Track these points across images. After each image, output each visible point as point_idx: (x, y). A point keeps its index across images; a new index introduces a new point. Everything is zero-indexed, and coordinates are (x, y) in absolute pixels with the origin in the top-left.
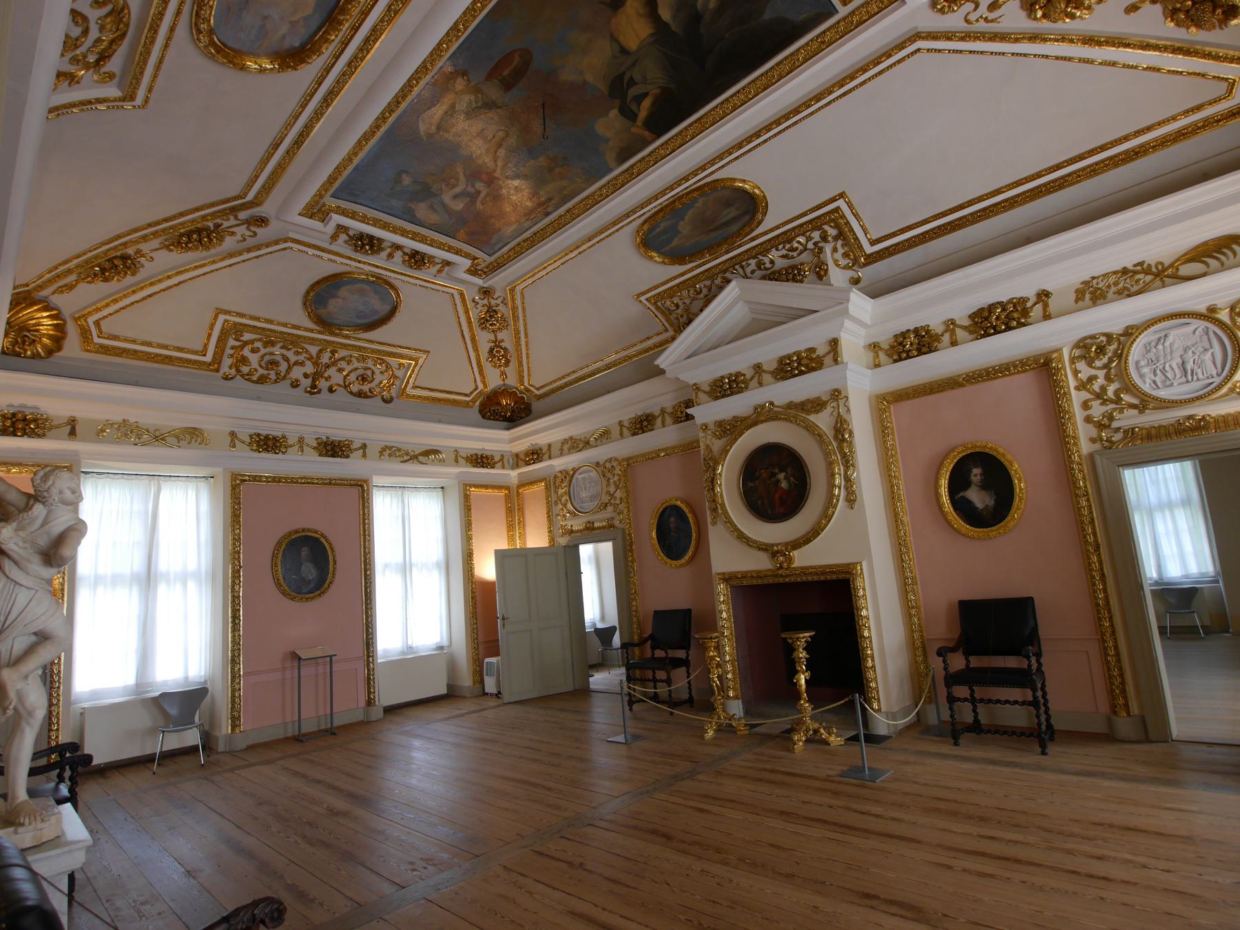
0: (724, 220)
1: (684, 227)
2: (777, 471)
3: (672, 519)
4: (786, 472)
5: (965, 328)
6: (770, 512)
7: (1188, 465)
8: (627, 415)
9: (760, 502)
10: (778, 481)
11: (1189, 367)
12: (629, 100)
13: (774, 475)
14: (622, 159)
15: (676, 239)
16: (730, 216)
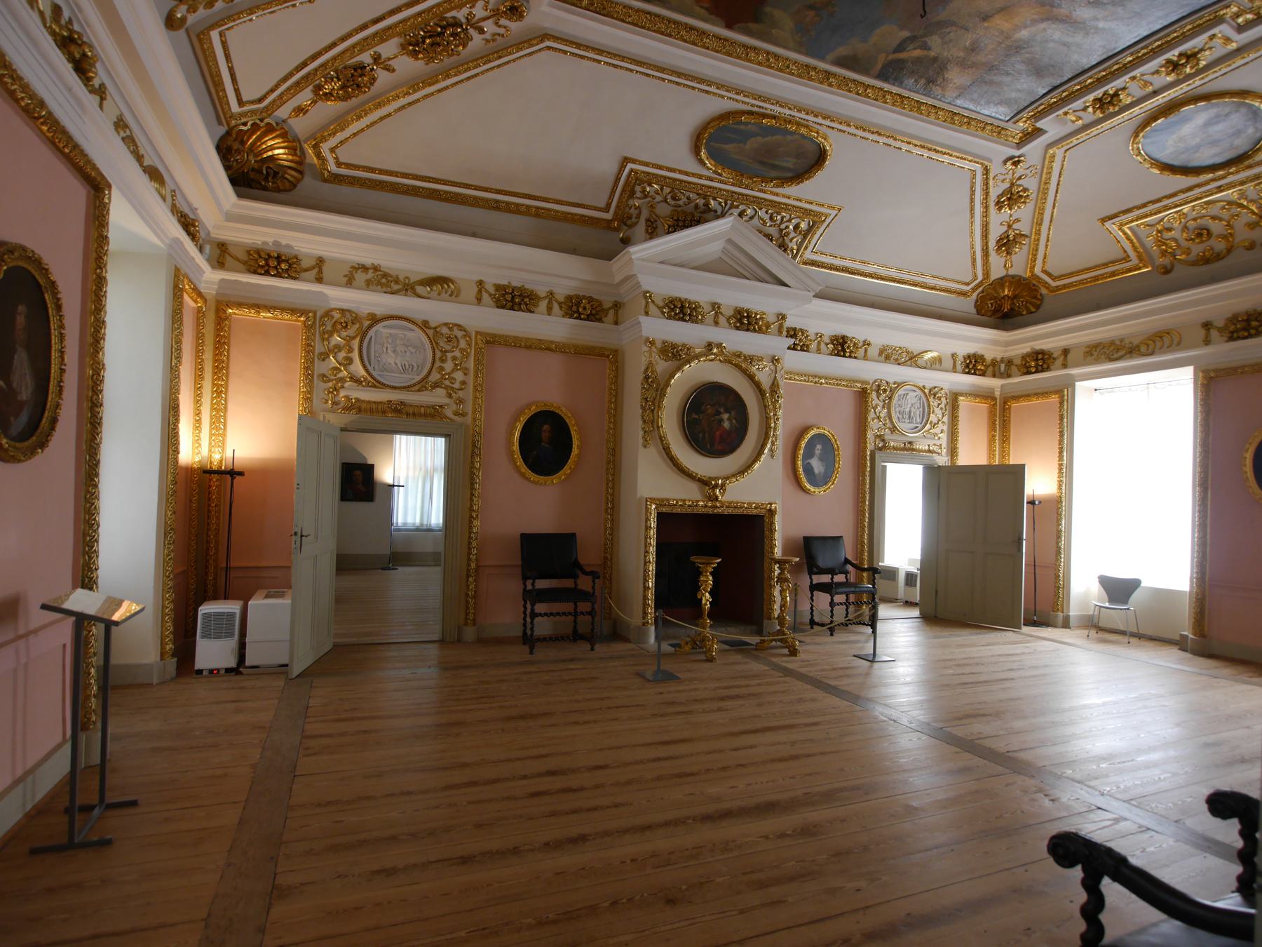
0: (777, 163)
1: (751, 144)
2: (722, 410)
3: (546, 427)
4: (729, 413)
5: (560, 304)
6: (709, 446)
7: (440, 442)
8: (494, 277)
9: (701, 435)
10: (721, 420)
11: (912, 414)
12: (923, 39)
13: (719, 413)
14: (840, 63)
15: (734, 145)
16: (785, 164)
